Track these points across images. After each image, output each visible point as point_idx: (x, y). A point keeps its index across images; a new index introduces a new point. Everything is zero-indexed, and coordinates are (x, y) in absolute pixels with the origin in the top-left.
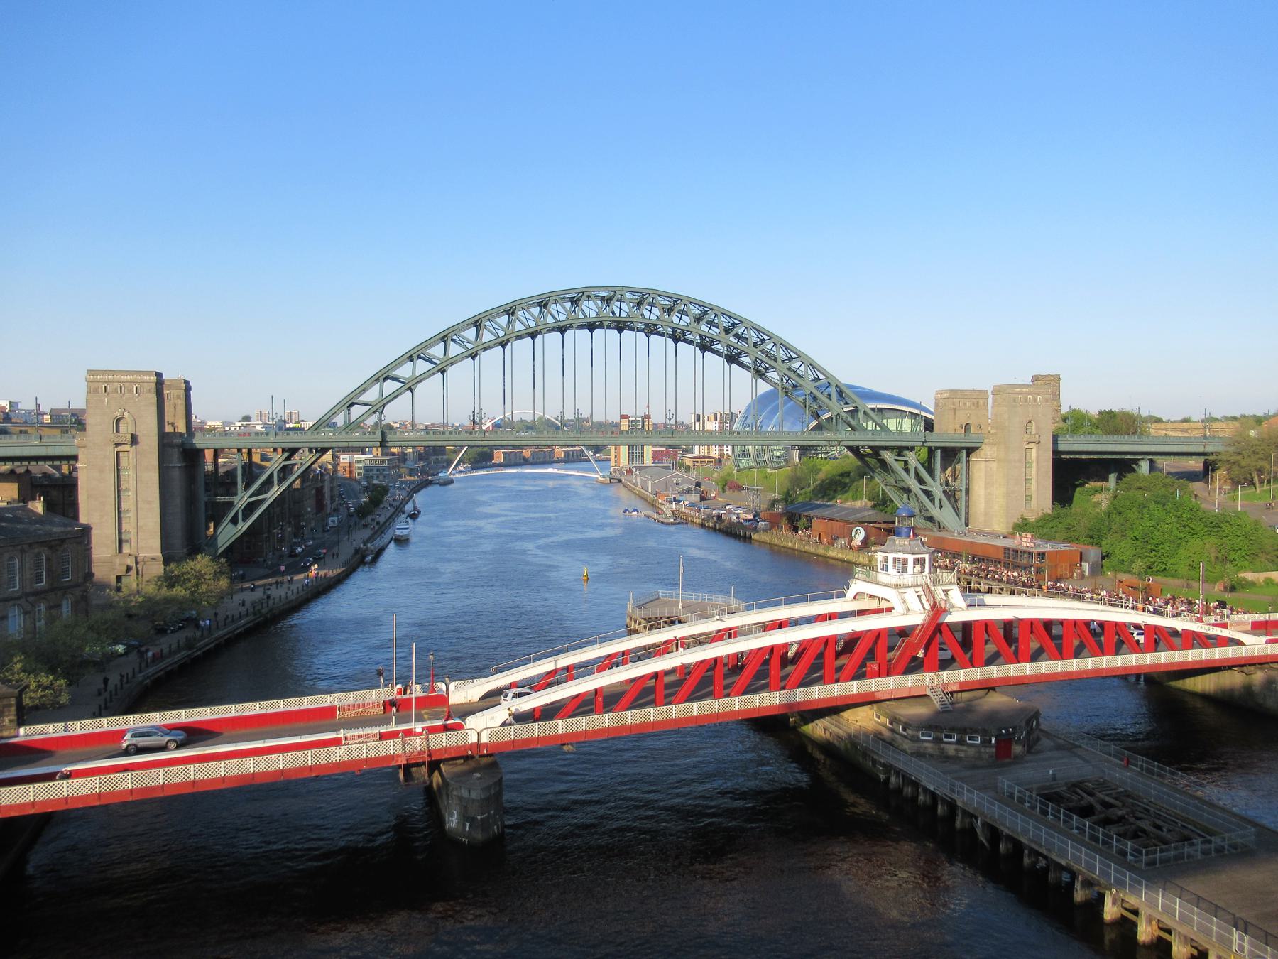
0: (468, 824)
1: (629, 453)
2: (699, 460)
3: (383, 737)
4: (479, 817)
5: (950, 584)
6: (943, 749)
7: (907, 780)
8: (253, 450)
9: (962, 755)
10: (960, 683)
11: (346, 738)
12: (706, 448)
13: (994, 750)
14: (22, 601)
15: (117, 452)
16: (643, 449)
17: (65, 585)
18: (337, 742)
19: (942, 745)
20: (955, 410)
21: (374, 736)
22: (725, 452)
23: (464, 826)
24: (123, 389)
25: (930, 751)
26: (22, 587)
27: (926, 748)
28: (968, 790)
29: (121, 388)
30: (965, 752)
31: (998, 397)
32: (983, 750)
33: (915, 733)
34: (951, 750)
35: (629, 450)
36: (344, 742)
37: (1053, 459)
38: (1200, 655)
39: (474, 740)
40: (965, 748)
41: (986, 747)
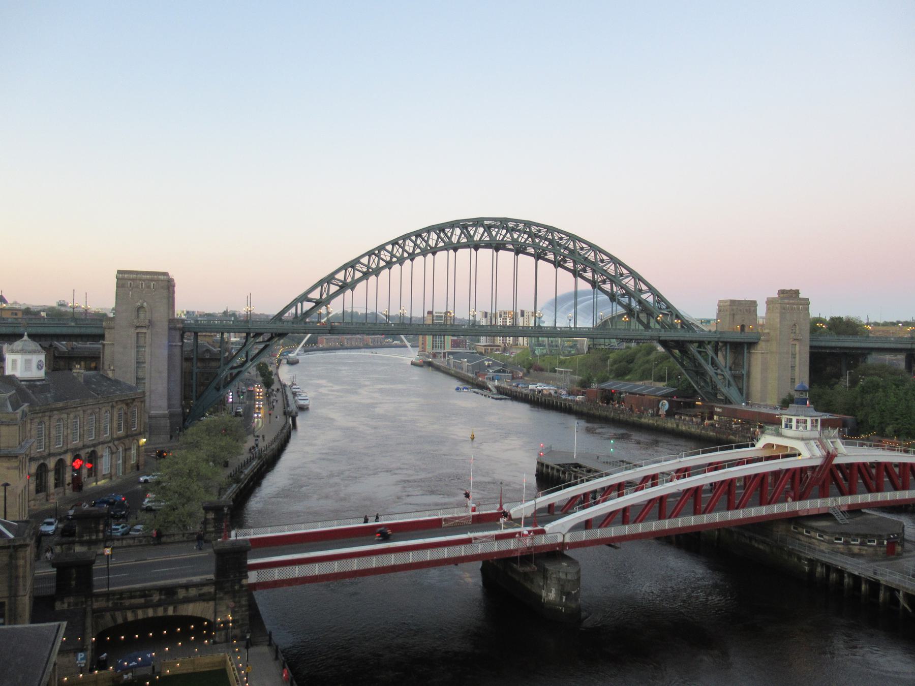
0: (564, 597)
1: (433, 341)
2: (489, 348)
3: (499, 537)
4: (573, 592)
5: (834, 437)
6: (850, 549)
7: (829, 567)
8: (199, 334)
9: (864, 552)
10: (849, 506)
11: (476, 539)
12: (492, 338)
13: (885, 549)
14: (111, 445)
15: (138, 333)
16: (444, 338)
17: (135, 432)
18: (468, 541)
19: (851, 546)
20: (734, 315)
21: (492, 537)
22: (508, 342)
23: (561, 598)
24: (144, 285)
25: (841, 550)
26: (112, 434)
27: (838, 548)
28: (890, 573)
29: (142, 284)
30: (865, 550)
31: (771, 306)
32: (878, 549)
33: (831, 538)
34: (856, 549)
35: (433, 338)
36: (473, 541)
37: (810, 352)
38: (886, 497)
39: (560, 540)
40: (866, 548)
41: (881, 547)
